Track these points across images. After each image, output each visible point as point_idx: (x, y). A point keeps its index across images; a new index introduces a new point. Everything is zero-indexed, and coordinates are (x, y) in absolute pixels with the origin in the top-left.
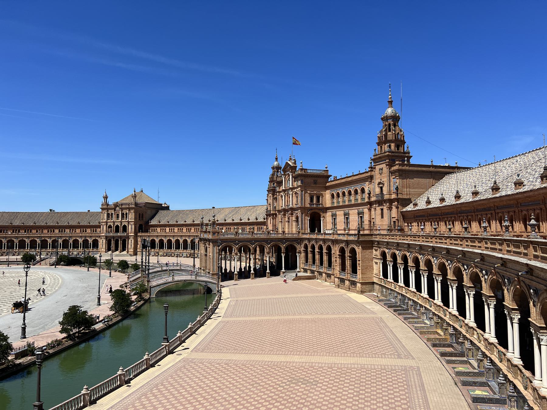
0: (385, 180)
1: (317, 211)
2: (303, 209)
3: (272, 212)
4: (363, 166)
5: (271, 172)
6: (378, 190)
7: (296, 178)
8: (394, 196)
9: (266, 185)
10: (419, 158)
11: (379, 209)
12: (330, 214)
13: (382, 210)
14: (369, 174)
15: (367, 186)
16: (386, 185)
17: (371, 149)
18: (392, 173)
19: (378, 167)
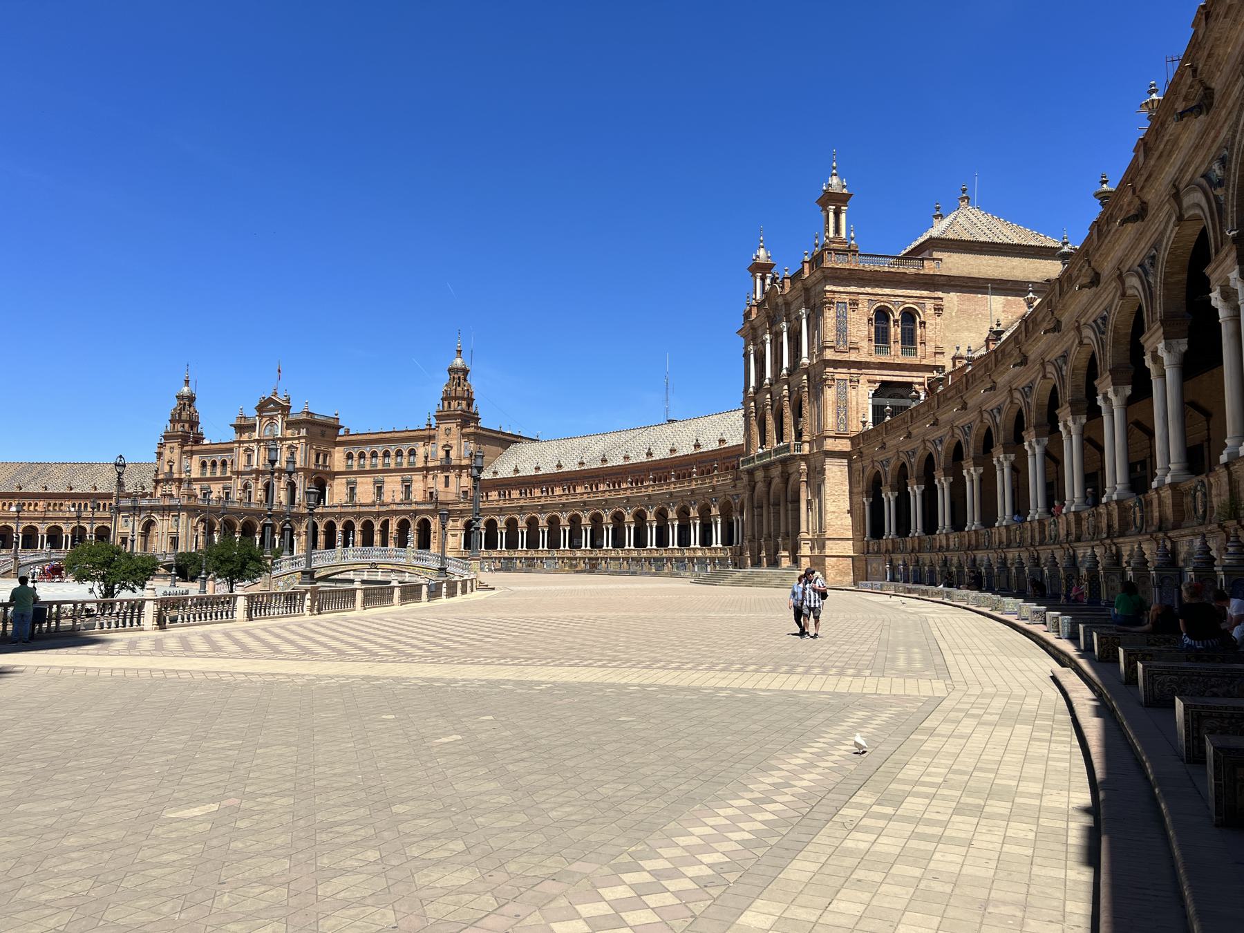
0: (454, 442)
1: (322, 476)
2: (305, 470)
3: (176, 476)
4: (418, 421)
5: (175, 403)
6: (442, 454)
7: (290, 425)
8: (464, 463)
9: (163, 424)
10: (488, 421)
11: (441, 477)
12: (344, 481)
13: (447, 477)
14: (427, 433)
15: (421, 450)
16: (455, 448)
17: (434, 403)
18: (463, 435)
19: (443, 427)
